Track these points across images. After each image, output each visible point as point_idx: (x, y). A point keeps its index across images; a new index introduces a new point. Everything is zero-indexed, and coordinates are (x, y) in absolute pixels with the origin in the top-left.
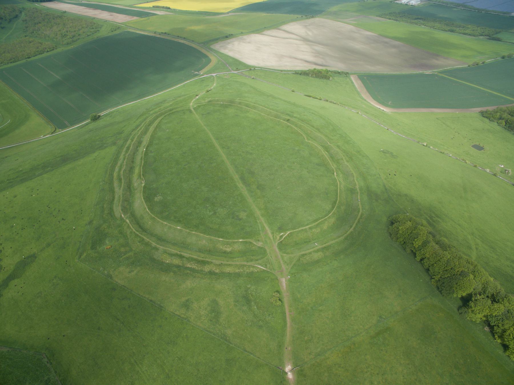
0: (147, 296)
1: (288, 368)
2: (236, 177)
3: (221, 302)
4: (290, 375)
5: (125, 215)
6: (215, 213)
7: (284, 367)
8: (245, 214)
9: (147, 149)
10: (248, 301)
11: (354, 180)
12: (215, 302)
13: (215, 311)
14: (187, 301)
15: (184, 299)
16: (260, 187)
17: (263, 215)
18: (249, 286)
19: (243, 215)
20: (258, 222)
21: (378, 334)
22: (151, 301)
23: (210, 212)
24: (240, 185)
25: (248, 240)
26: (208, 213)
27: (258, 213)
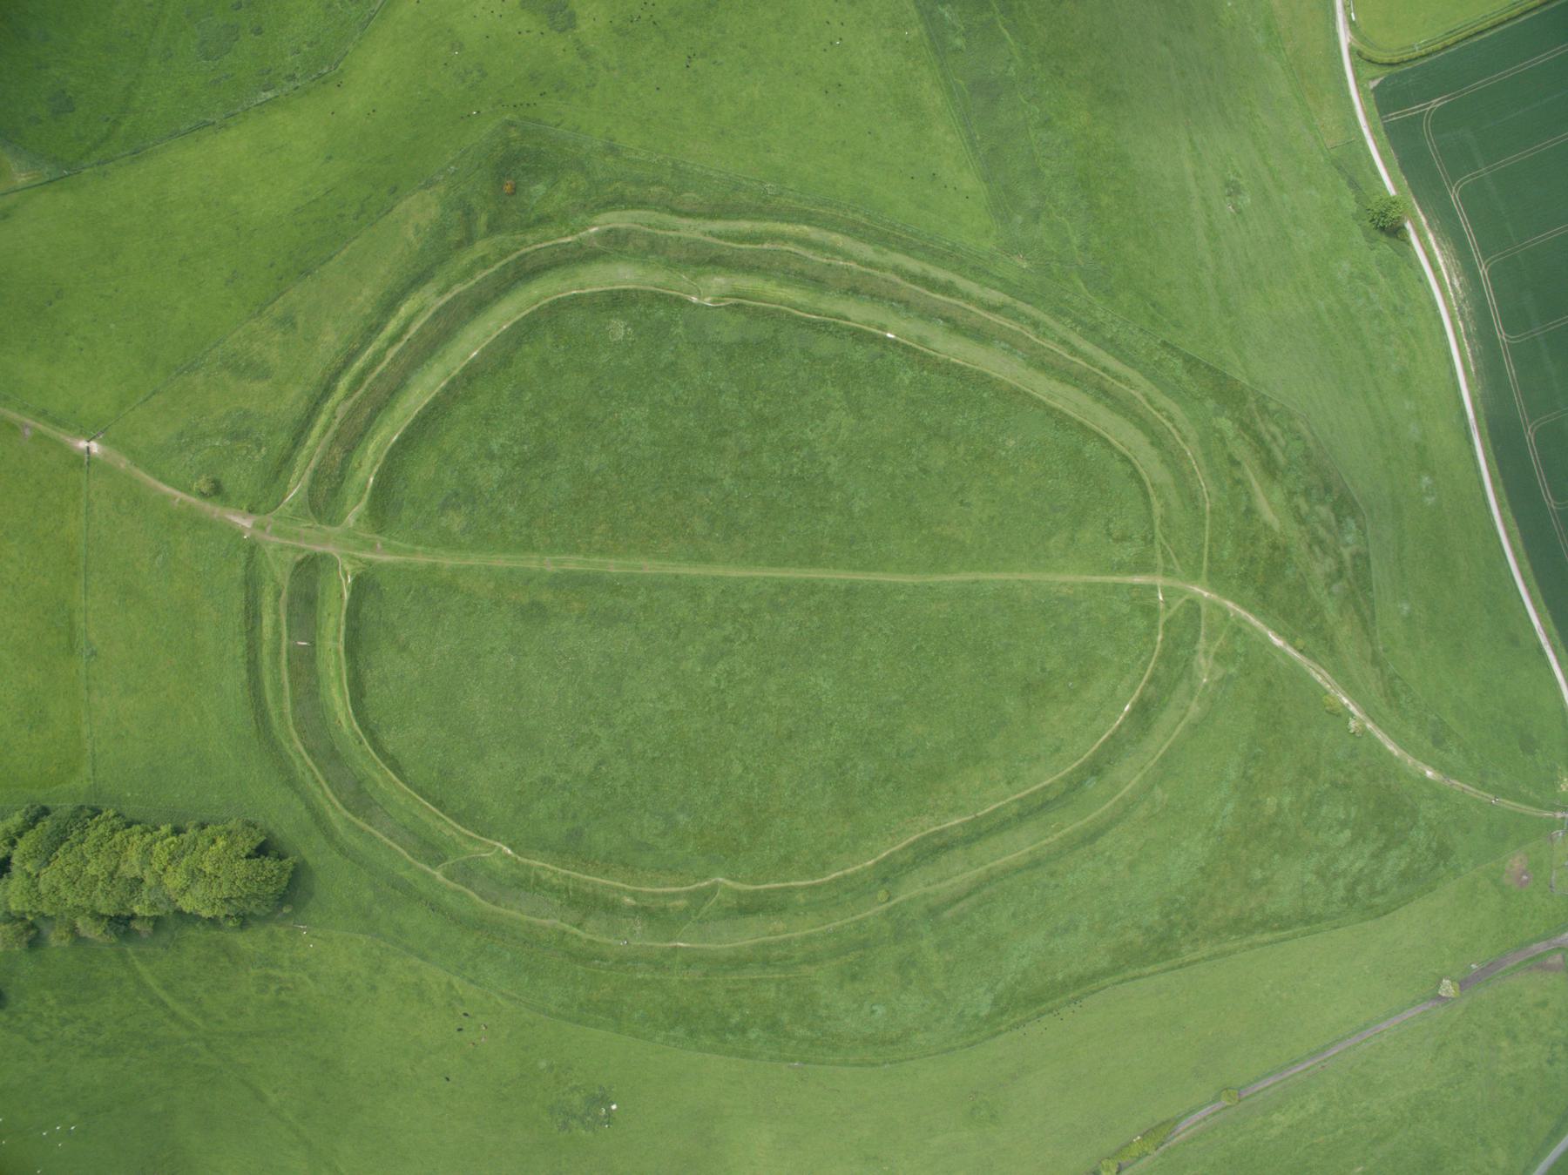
0: (344, 252)
1: (95, 447)
2: (613, 566)
3: (259, 386)
4: (83, 444)
5: (596, 234)
6: (491, 456)
7: (100, 442)
8: (455, 529)
9: (895, 343)
10: (236, 436)
11: (468, 885)
12: (266, 375)
13: (253, 369)
14: (294, 325)
15: (300, 319)
16: (535, 613)
17: (433, 568)
18: (263, 450)
19: (455, 522)
20: (419, 548)
21: (72, 625)
22: (331, 258)
23: (502, 446)
24: (573, 563)
25: (366, 497)
26: (501, 441)
27: (448, 561)
